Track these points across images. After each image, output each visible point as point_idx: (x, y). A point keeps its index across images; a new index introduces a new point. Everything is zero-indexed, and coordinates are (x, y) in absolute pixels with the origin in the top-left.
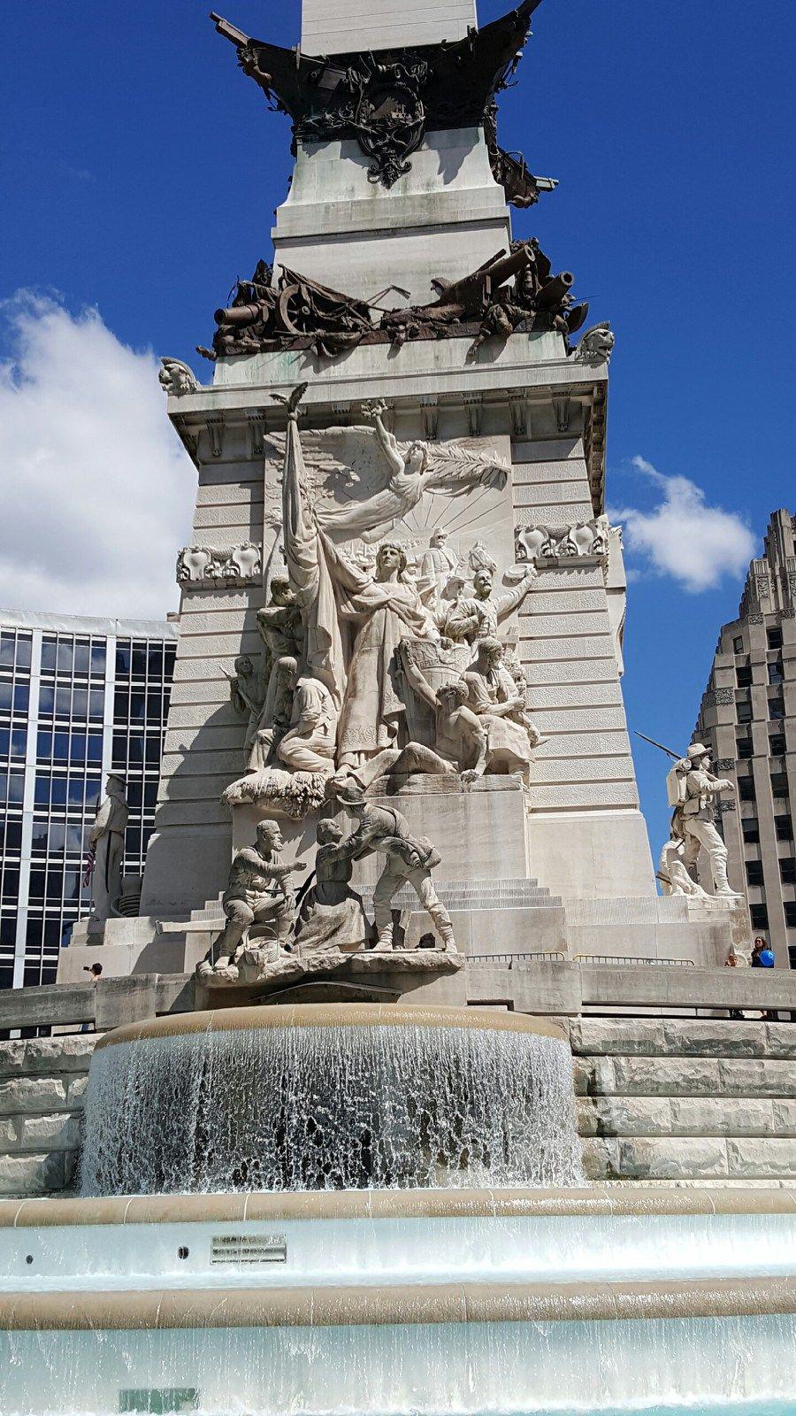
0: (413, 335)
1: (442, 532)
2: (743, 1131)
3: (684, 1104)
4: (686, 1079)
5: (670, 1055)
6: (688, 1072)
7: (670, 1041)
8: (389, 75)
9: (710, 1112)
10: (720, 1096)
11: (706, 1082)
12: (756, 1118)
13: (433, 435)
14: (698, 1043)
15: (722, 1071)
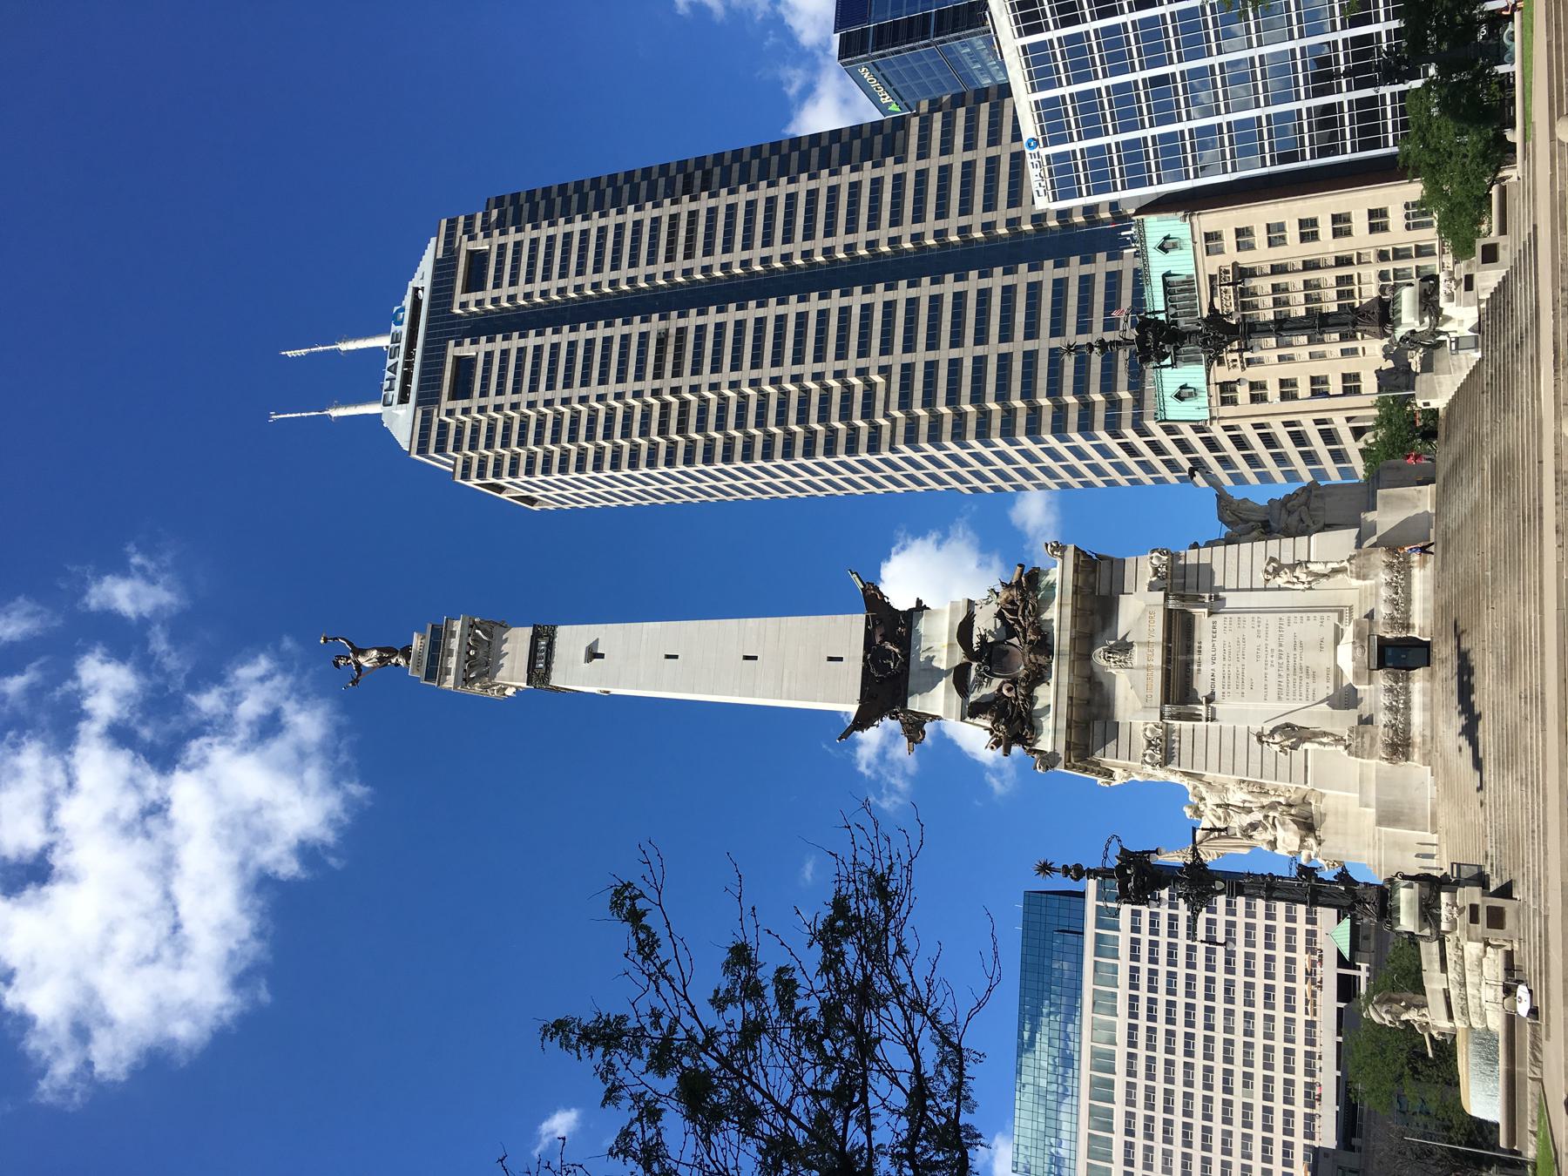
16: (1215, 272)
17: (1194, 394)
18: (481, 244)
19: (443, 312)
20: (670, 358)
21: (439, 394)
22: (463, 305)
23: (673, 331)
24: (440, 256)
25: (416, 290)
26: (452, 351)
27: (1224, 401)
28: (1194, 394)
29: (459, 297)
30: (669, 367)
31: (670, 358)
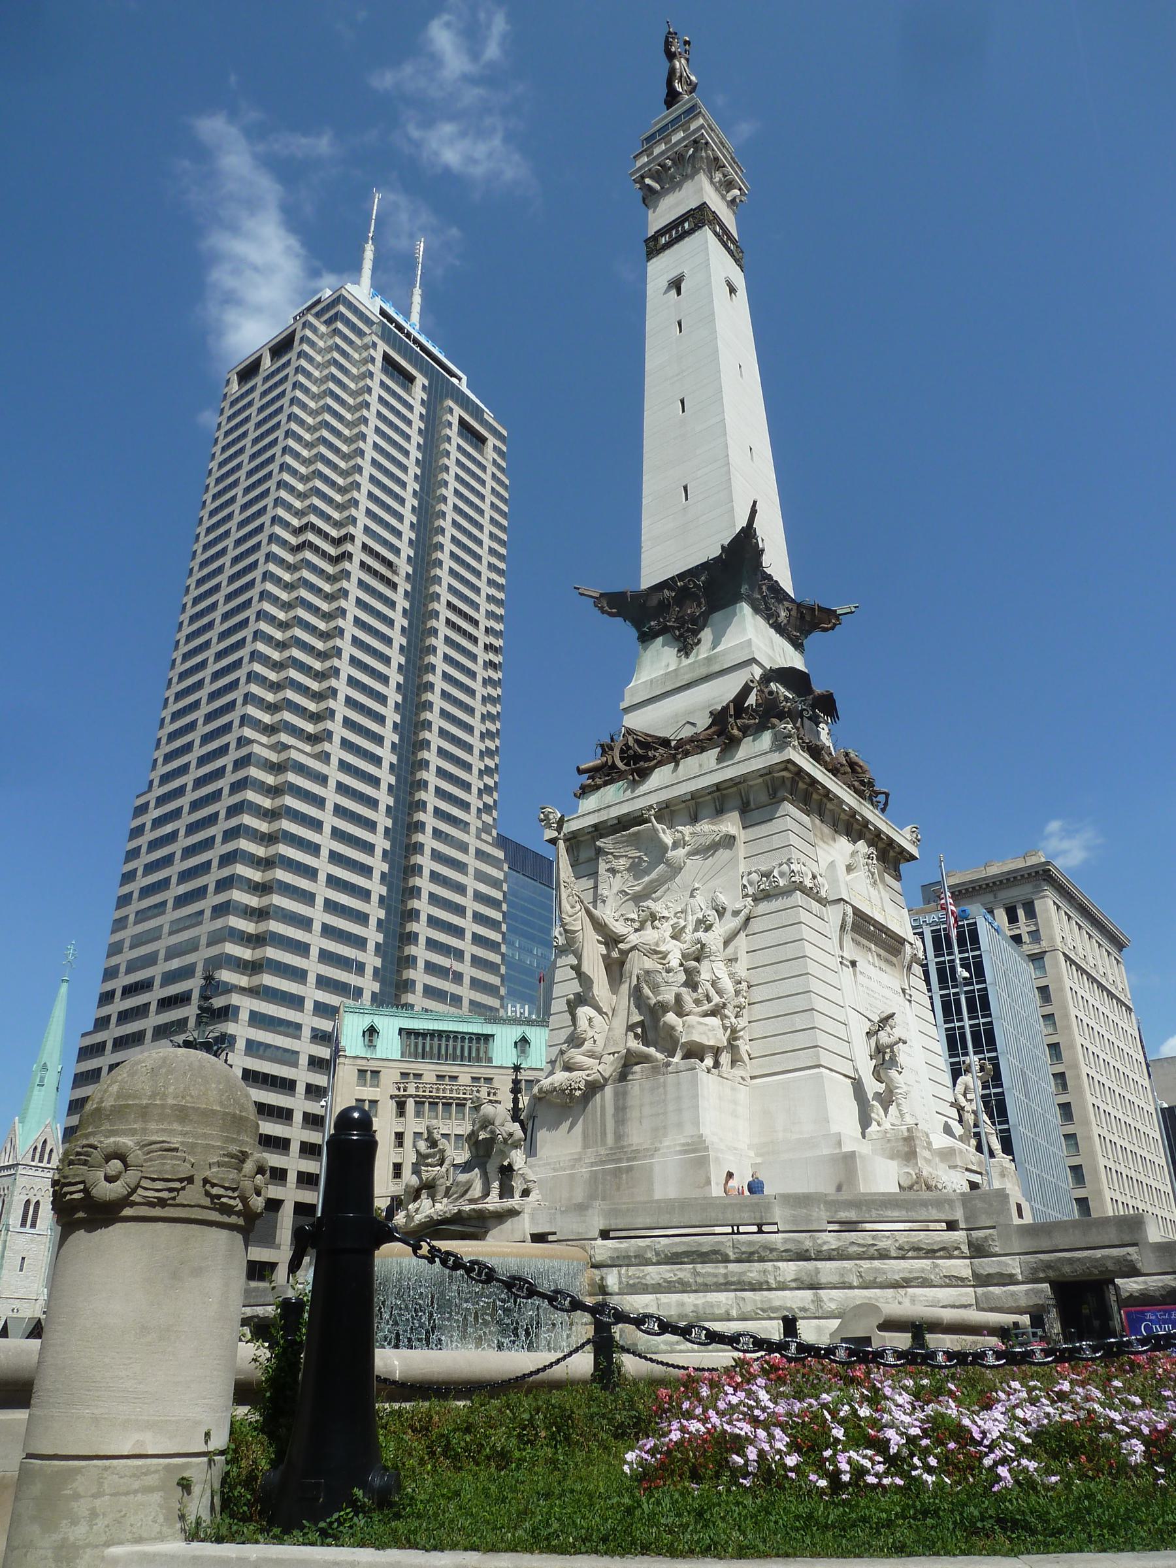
0: (687, 754)
1: (697, 886)
2: (710, 1317)
3: (664, 1298)
4: (666, 1281)
5: (658, 1263)
6: (668, 1276)
7: (657, 1254)
8: (685, 588)
9: (683, 1304)
10: (695, 1291)
11: (681, 1282)
12: (719, 1307)
13: (694, 819)
14: (676, 1254)
15: (696, 1274)
16: (495, 1084)
17: (371, 1045)
18: (490, 453)
19: (447, 391)
20: (377, 566)
21: (393, 348)
22: (451, 411)
23: (395, 579)
24: (486, 416)
25: (460, 379)
26: (421, 380)
27: (362, 1072)
28: (371, 1045)
29: (458, 411)
30: (370, 561)
31: (377, 566)
